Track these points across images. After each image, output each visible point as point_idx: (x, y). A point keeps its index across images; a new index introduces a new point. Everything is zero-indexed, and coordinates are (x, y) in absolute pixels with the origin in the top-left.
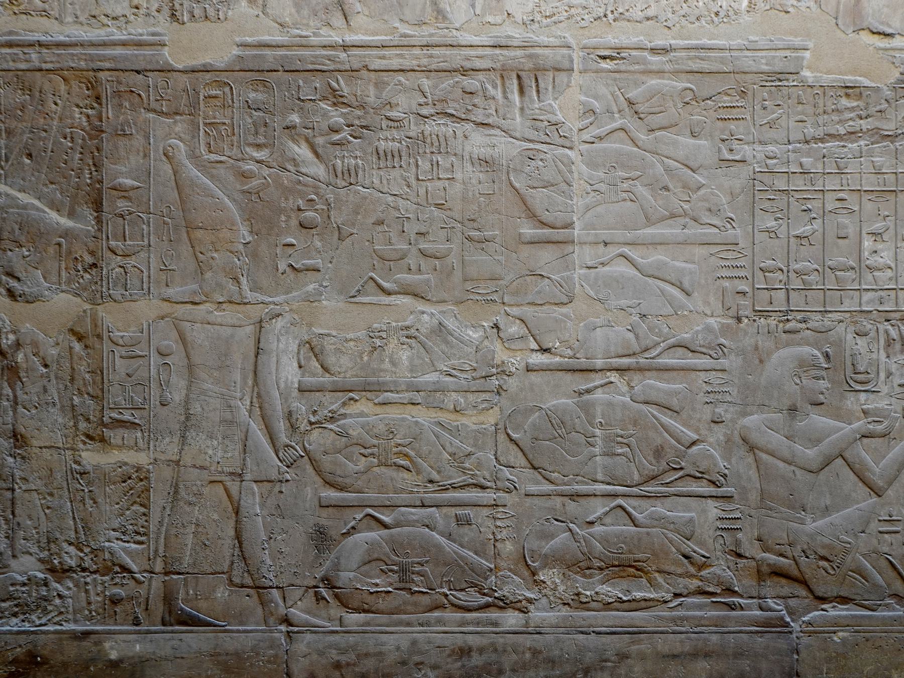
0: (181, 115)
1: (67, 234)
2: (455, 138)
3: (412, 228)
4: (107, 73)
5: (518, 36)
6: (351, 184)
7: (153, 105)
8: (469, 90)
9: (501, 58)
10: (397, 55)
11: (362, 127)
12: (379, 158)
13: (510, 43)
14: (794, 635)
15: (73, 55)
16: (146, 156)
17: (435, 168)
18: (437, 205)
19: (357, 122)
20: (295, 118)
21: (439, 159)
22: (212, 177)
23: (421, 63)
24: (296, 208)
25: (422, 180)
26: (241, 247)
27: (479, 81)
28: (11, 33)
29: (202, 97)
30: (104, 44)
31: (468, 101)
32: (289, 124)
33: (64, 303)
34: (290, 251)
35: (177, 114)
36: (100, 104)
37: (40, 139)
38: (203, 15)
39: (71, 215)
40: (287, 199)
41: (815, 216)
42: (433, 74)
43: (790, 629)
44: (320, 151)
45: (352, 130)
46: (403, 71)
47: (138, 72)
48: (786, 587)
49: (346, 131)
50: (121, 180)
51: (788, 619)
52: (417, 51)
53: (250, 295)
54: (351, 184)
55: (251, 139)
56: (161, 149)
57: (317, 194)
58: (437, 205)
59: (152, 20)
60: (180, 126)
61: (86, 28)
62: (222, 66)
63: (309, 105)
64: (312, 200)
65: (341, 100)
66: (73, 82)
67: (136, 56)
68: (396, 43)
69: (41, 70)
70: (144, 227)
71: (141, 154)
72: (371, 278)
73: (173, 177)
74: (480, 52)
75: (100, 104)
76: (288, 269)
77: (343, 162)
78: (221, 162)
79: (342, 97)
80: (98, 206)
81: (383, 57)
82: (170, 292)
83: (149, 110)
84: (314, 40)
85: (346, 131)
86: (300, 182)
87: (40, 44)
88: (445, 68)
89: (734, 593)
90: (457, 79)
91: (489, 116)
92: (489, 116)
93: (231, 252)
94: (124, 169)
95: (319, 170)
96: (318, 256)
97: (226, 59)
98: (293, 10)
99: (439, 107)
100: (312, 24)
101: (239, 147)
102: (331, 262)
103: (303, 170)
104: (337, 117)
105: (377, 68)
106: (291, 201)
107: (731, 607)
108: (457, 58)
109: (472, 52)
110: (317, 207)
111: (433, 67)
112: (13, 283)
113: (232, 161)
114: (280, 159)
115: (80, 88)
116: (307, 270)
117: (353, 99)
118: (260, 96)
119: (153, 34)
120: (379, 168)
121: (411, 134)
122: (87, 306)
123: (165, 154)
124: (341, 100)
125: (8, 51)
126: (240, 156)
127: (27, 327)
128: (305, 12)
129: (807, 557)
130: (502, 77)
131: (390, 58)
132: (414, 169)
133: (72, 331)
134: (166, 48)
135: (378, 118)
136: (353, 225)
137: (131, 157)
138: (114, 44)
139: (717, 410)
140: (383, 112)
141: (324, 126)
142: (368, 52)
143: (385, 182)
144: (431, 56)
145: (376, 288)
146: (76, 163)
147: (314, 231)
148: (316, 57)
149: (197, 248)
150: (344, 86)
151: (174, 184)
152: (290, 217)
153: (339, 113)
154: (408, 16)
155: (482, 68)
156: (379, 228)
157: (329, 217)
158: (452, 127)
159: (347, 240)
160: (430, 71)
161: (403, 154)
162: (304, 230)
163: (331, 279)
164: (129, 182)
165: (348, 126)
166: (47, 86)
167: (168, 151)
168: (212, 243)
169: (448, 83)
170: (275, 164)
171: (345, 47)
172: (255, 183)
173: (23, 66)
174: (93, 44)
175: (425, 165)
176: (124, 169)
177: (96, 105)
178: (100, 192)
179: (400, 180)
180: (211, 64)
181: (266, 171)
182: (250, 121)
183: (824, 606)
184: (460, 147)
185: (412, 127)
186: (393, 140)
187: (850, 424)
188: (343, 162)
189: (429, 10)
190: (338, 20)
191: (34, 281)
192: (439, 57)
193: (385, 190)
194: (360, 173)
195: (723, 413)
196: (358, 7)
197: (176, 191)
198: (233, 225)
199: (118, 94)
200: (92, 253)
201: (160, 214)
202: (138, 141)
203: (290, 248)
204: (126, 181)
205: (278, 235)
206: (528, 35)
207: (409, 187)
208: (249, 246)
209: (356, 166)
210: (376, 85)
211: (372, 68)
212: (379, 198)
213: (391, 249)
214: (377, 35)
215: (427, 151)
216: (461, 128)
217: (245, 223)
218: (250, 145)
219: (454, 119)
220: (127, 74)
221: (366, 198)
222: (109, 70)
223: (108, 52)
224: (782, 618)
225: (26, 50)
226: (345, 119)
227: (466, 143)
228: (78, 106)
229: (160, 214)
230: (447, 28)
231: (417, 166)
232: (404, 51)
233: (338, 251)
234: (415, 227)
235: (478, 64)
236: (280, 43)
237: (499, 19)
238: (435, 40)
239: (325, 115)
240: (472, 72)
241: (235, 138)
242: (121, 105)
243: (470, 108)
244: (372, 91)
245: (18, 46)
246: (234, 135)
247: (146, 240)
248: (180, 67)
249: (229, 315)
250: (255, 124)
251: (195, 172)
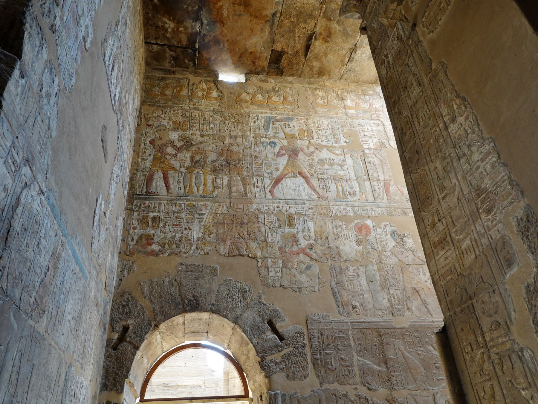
1: (379, 371)
20: (427, 340)
22: (412, 355)
33: (382, 391)
39: (379, 366)
53: (430, 388)
80: (386, 363)
82: (410, 387)
112: (369, 386)
122: (389, 392)
127: (375, 399)
133: (386, 399)
138: (381, 322)
146: (378, 352)
164: (392, 357)
171: (433, 322)
178: (386, 360)
181: (424, 354)
190: (430, 316)
191: (374, 386)
196: (433, 313)
200: (387, 377)
202: (392, 346)
223: (380, 324)
249: (425, 393)
251: (407, 354)
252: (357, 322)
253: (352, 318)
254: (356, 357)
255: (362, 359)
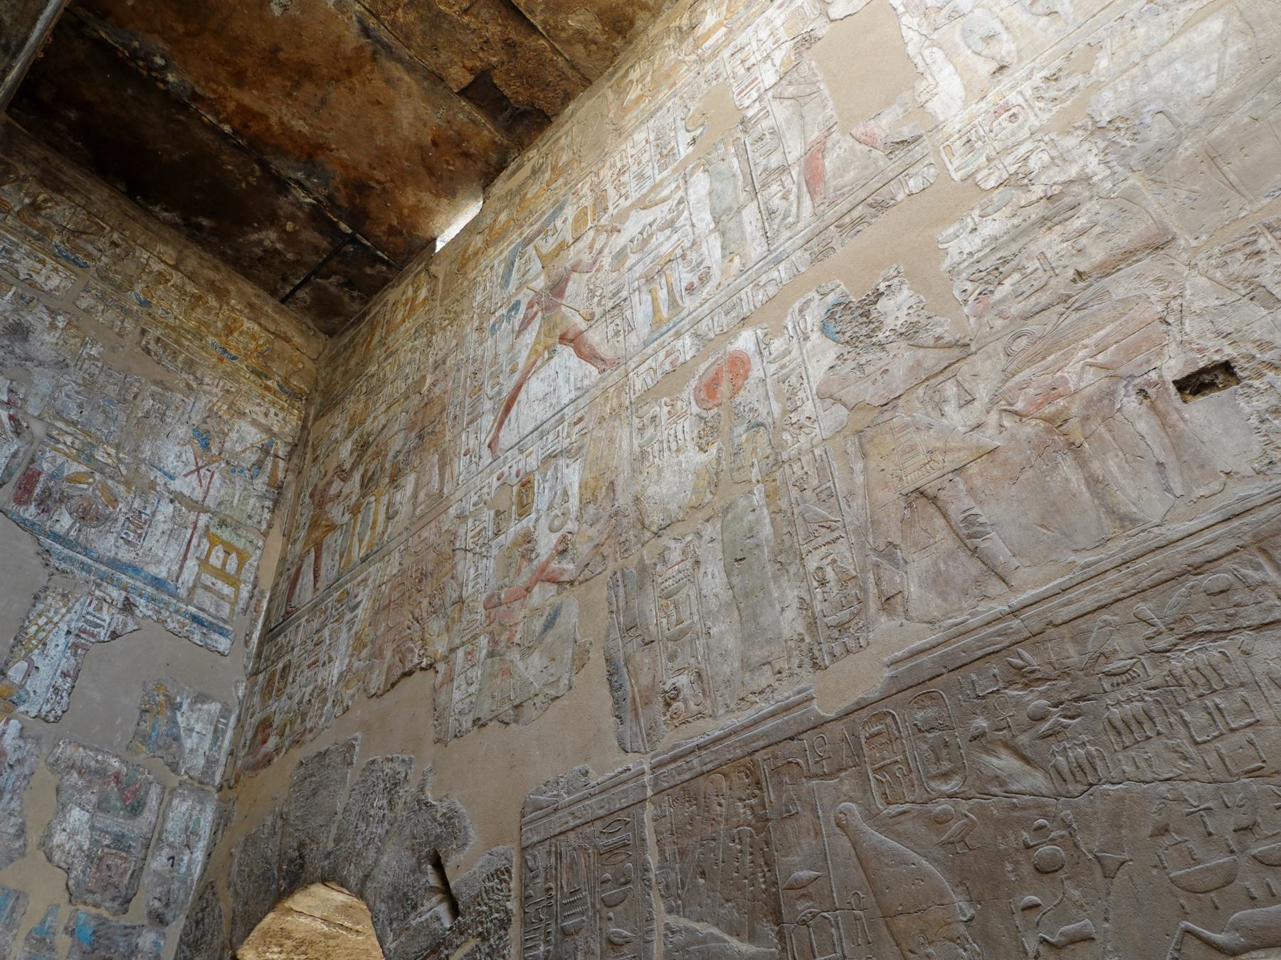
0: (845, 770)
2: (1229, 661)
3: (1223, 825)
4: (762, 752)
5: (1255, 492)
6: (1091, 785)
7: (814, 769)
8: (1217, 590)
9: (1246, 528)
10: (1087, 592)
11: (1077, 700)
12: (1119, 733)
13: (1249, 505)
15: (728, 746)
16: (818, 834)
17: (1217, 717)
18: (1249, 773)
19: (1066, 696)
20: (981, 723)
21: (1218, 701)
22: (899, 836)
23: (1126, 587)
24: (1022, 845)
25: (1205, 742)
26: (962, 929)
27: (1226, 571)
28: (674, 747)
29: (863, 740)
30: (755, 723)
31: (1222, 604)
32: (976, 733)
34: (1035, 916)
35: (840, 770)
36: (761, 789)
37: (711, 850)
38: (843, 650)
40: (1005, 837)
42: (1148, 593)
44: (1028, 753)
45: (1064, 709)
46: (1104, 607)
47: (792, 739)
49: (1055, 713)
50: (796, 874)
52: (1113, 576)
54: (1091, 785)
55: (933, 770)
56: (832, 819)
57: (1045, 816)
58: (1249, 773)
59: (796, 679)
60: (847, 784)
61: (737, 713)
62: (876, 695)
63: (992, 700)
64: (1041, 827)
65: (1033, 676)
66: (732, 775)
67: (787, 722)
68: (1080, 579)
69: (703, 774)
70: (833, 930)
71: (812, 833)
72: (1188, 931)
73: (853, 852)
74: (1208, 536)
75: (761, 789)
76: (1042, 949)
77: (1067, 757)
78: (904, 812)
79: (1032, 672)
80: (777, 918)
81: (1070, 603)
83: (810, 777)
84: (974, 622)
85: (1055, 713)
86: (1014, 807)
87: (700, 747)
88: (1164, 578)
90: (1190, 584)
91: (1270, 609)
92: (1270, 609)
93: (951, 940)
94: (797, 859)
95: (1037, 780)
96: (1082, 914)
97: (879, 686)
98: (939, 601)
99: (1181, 630)
100: (965, 605)
101: (922, 784)
102: (1106, 920)
103: (1015, 788)
104: (1035, 700)
105: (1066, 618)
106: (1012, 838)
108: (1177, 558)
109: (1196, 541)
110: (1053, 835)
111: (1145, 583)
113: (918, 807)
114: (977, 783)
115: (740, 778)
116: (1073, 942)
117: (1049, 669)
118: (930, 713)
119: (799, 693)
120: (1125, 748)
121: (1154, 682)
123: (838, 825)
124: (1033, 676)
125: (673, 765)
126: (925, 796)
128: (954, 597)
130: (1263, 550)
131: (1079, 600)
132: (1182, 730)
134: (815, 701)
135: (1094, 680)
136: (1119, 847)
137: (802, 841)
138: (764, 719)
140: (1098, 669)
141: (1023, 717)
142: (1046, 605)
143: (1142, 764)
144: (1136, 573)
145: (1204, 947)
147: (1061, 875)
148: (982, 639)
149: (904, 946)
150: (1029, 658)
151: (856, 860)
152: (1017, 863)
153: (1036, 694)
154: (1082, 541)
155: (1221, 552)
156: (1166, 841)
157: (1076, 846)
158: (1215, 648)
159: (1119, 875)
160: (1144, 591)
161: (1154, 713)
162: (1045, 878)
163: (1117, 949)
164: (805, 874)
165: (1056, 706)
166: (710, 790)
167: (840, 819)
168: (922, 932)
169: (1178, 593)
170: (973, 792)
171: (1014, 613)
172: (955, 826)
173: (686, 776)
174: (745, 727)
175: (1198, 718)
176: (797, 859)
177: (757, 792)
179: (1166, 754)
180: (864, 699)
181: (964, 806)
182: (925, 747)
184: (1245, 671)
185: (1151, 672)
186: (1130, 700)
188: (1067, 757)
189: (1107, 522)
190: (995, 587)
192: (1148, 569)
193: (1149, 776)
194: (1099, 763)
197: (861, 870)
198: (942, 897)
199: (776, 771)
201: (848, 906)
202: (806, 818)
203: (1034, 911)
204: (801, 873)
205: (1009, 896)
206: (1274, 482)
207: (1186, 759)
208: (974, 923)
209: (1089, 756)
210: (1073, 639)
211: (1060, 621)
212: (1144, 791)
213: (1201, 871)
214: (1051, 581)
215: (1192, 696)
216: (1230, 646)
217: (959, 890)
218: (934, 777)
219: (1214, 636)
220: (781, 745)
221: (1123, 798)
222: (763, 748)
225: (688, 759)
226: (1047, 698)
227: (1252, 662)
228: (741, 800)
229: (848, 906)
230: (1143, 531)
231: (1185, 724)
232: (1096, 583)
233: (1111, 898)
234: (1231, 821)
235: (1213, 551)
236: (934, 643)
237: (1215, 486)
238: (1132, 551)
239: (1018, 703)
240: (1209, 565)
241: (913, 776)
242: (781, 783)
243: (1232, 611)
244: (1071, 649)
245: (681, 757)
246: (911, 771)
247: (838, 949)
248: (833, 715)
250: (932, 749)
252: (674, 759)
253: (659, 748)
254: (662, 917)
255: (683, 922)
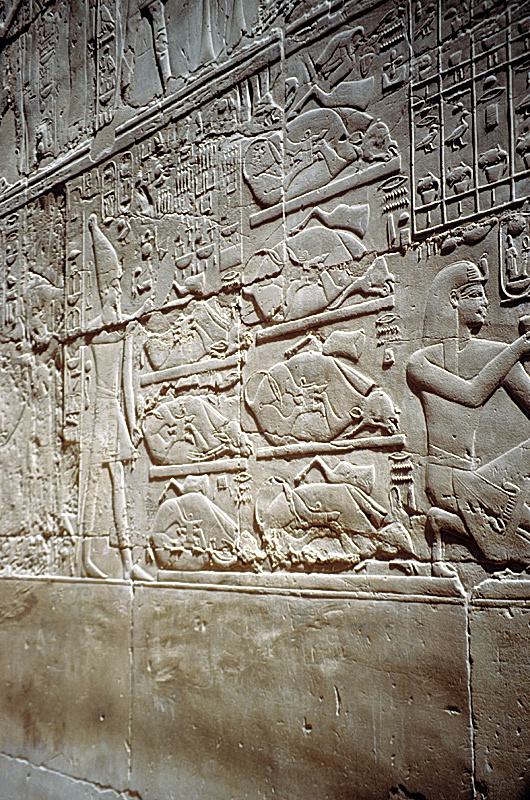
14: (466, 608)
41: (466, 112)
43: (460, 600)
48: (461, 551)
51: (460, 588)
89: (410, 556)
107: (402, 569)
129: (474, 511)
139: (387, 350)
183: (496, 573)
187: (510, 343)
195: (392, 353)
224: (452, 586)
